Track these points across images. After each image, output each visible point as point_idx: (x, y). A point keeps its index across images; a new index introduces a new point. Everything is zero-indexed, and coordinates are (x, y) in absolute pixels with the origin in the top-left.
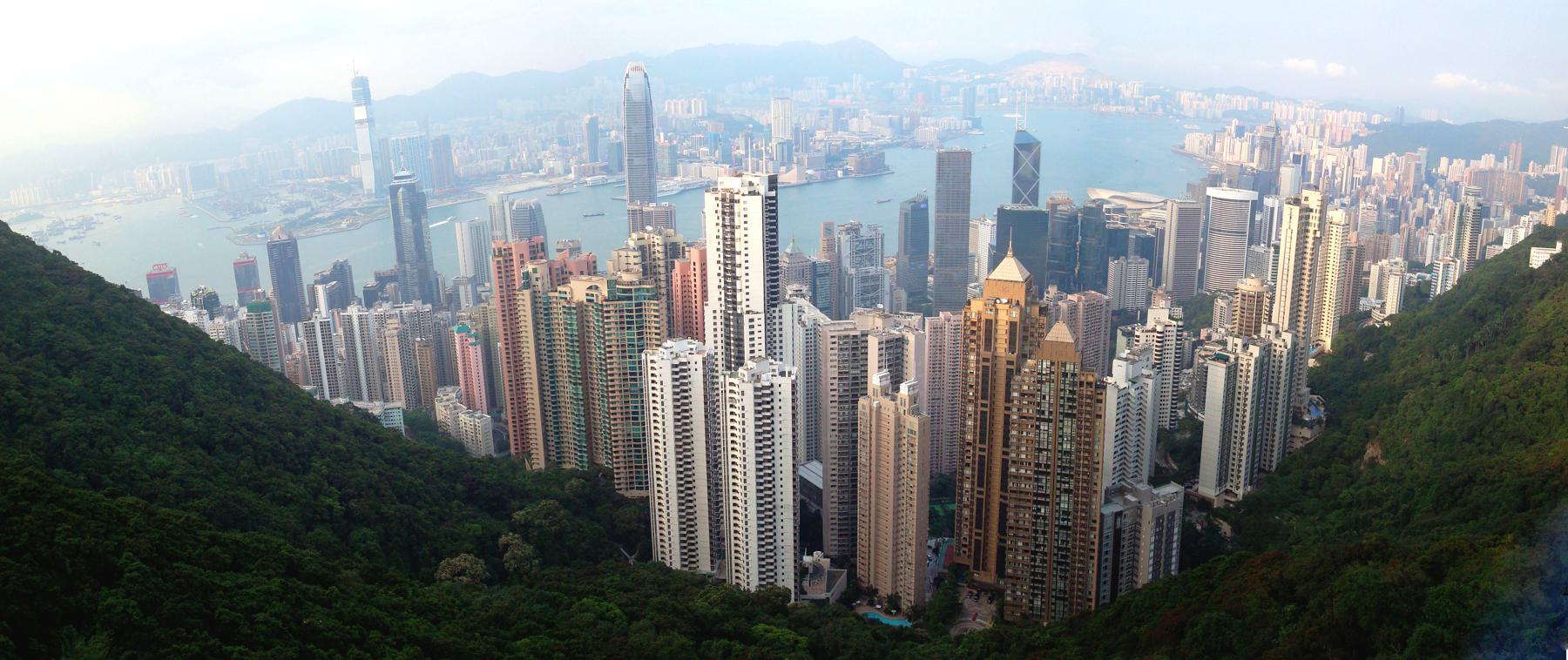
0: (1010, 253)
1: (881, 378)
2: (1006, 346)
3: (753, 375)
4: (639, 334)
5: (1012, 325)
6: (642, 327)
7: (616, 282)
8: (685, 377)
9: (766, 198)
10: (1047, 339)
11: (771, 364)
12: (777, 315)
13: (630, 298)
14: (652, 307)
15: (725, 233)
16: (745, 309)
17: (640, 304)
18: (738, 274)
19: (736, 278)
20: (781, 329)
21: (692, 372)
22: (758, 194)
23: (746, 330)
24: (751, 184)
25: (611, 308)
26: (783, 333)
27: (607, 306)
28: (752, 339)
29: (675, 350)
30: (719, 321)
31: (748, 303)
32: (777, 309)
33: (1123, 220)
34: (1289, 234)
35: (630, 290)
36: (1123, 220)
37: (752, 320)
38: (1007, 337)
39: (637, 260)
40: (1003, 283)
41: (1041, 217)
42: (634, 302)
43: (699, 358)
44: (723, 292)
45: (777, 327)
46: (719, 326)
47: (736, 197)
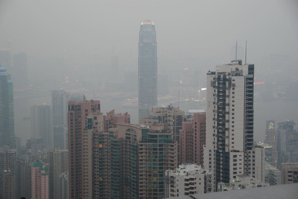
3: (240, 186)
4: (160, 164)
6: (162, 160)
7: (147, 130)
8: (192, 188)
9: (248, 79)
11: (252, 180)
12: (251, 154)
13: (156, 141)
14: (170, 147)
15: (219, 100)
16: (231, 149)
20: (254, 165)
21: (197, 185)
22: (242, 76)
23: (231, 162)
24: (237, 69)
25: (144, 147)
26: (256, 167)
27: (142, 145)
28: (235, 169)
29: (187, 170)
30: (213, 157)
31: (233, 145)
32: (251, 151)
35: (156, 136)
37: (235, 156)
42: (158, 144)
43: (202, 177)
44: (216, 138)
45: (251, 163)
46: (213, 161)
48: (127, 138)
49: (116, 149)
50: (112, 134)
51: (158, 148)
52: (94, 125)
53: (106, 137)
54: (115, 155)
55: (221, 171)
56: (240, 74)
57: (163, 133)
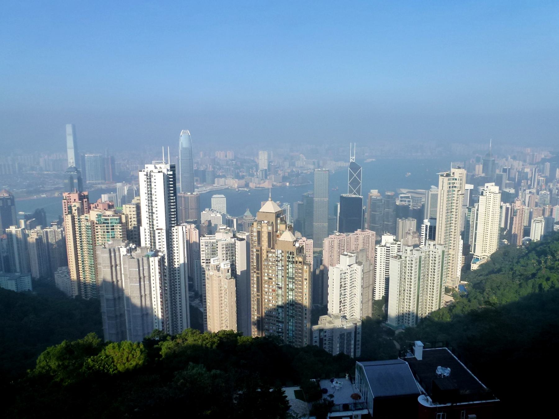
0: (270, 199)
1: (214, 260)
2: (267, 244)
5: (269, 233)
10: (280, 239)
13: (108, 223)
17: (113, 226)
18: (154, 211)
19: (153, 213)
23: (157, 238)
24: (160, 168)
27: (97, 227)
30: (148, 234)
33: (409, 201)
34: (442, 193)
35: (108, 219)
36: (409, 201)
37: (159, 233)
38: (267, 239)
39: (135, 209)
40: (265, 214)
41: (361, 199)
42: (110, 225)
44: (148, 219)
46: (148, 237)
47: (152, 174)
48: (97, 220)
49: (88, 229)
50: (87, 218)
51: (110, 228)
52: (74, 211)
53: (83, 220)
54: (88, 234)
55: (153, 244)
56: (162, 171)
57: (113, 216)
